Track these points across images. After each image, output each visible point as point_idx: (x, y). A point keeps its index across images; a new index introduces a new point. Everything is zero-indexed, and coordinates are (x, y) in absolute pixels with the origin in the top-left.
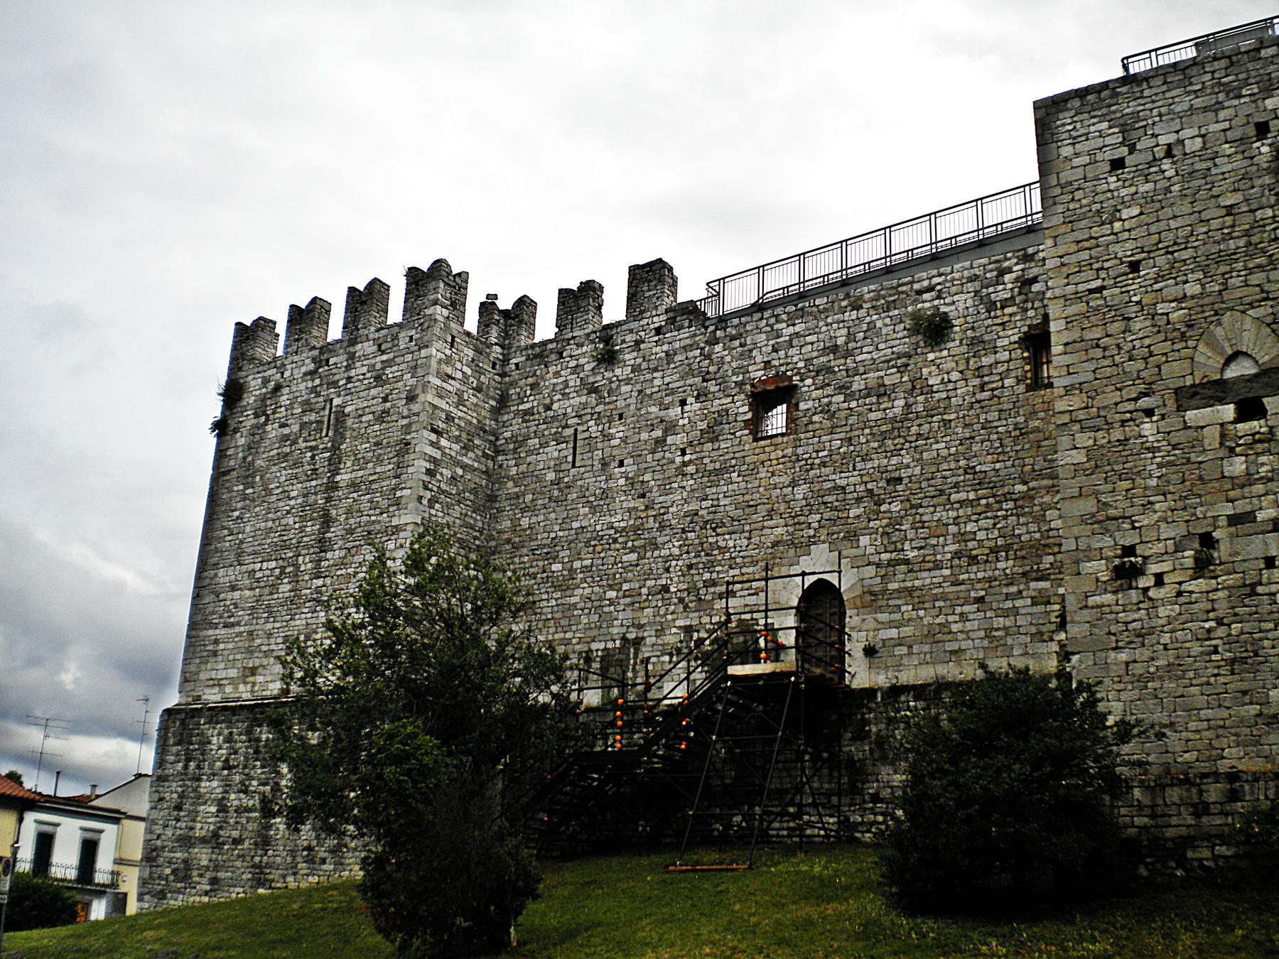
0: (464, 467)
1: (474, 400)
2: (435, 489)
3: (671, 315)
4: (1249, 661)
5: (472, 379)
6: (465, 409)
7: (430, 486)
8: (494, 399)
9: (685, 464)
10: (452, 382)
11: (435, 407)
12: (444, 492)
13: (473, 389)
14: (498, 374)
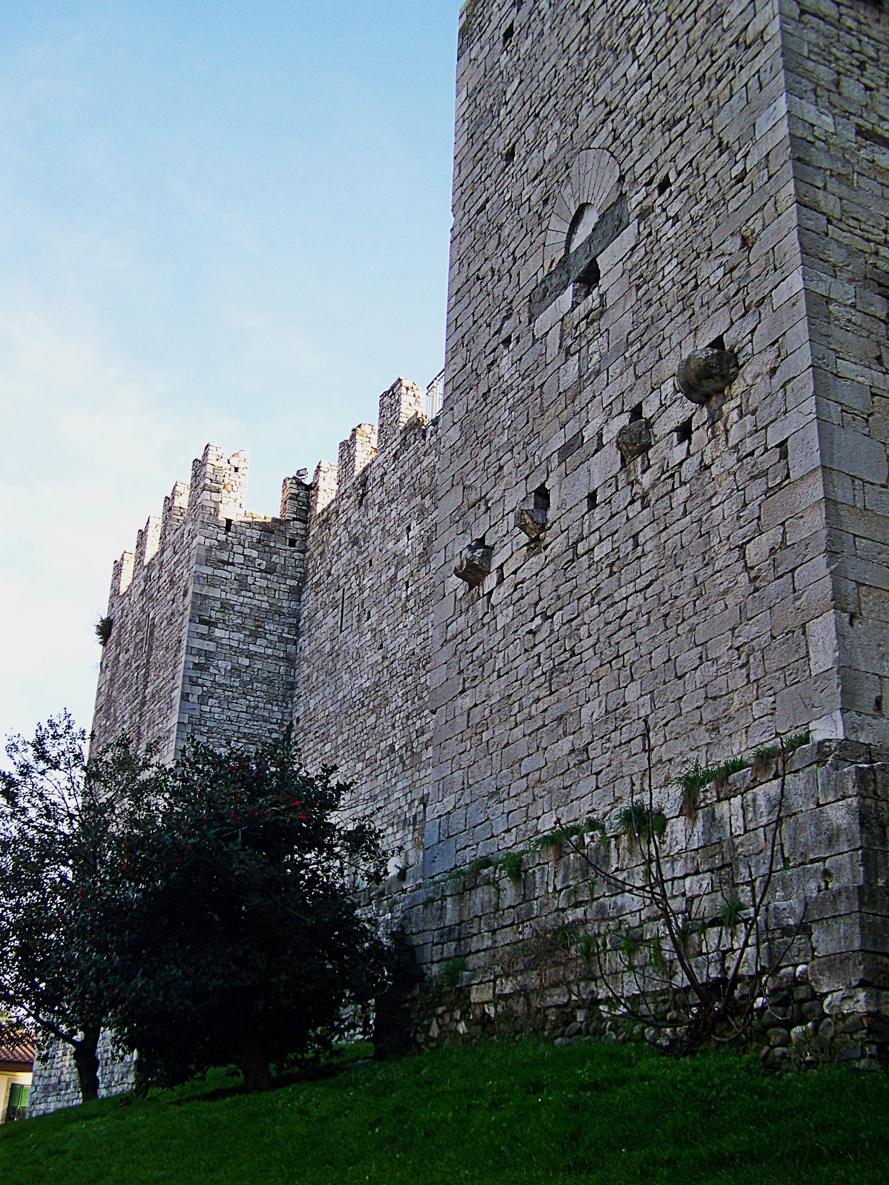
0: (250, 656)
1: (264, 583)
2: (208, 684)
3: (403, 435)
4: (566, 666)
5: (258, 561)
6: (251, 594)
7: (200, 681)
8: (293, 578)
9: (408, 599)
10: (230, 568)
11: (206, 597)
12: (220, 685)
13: (261, 571)
14: (299, 551)
